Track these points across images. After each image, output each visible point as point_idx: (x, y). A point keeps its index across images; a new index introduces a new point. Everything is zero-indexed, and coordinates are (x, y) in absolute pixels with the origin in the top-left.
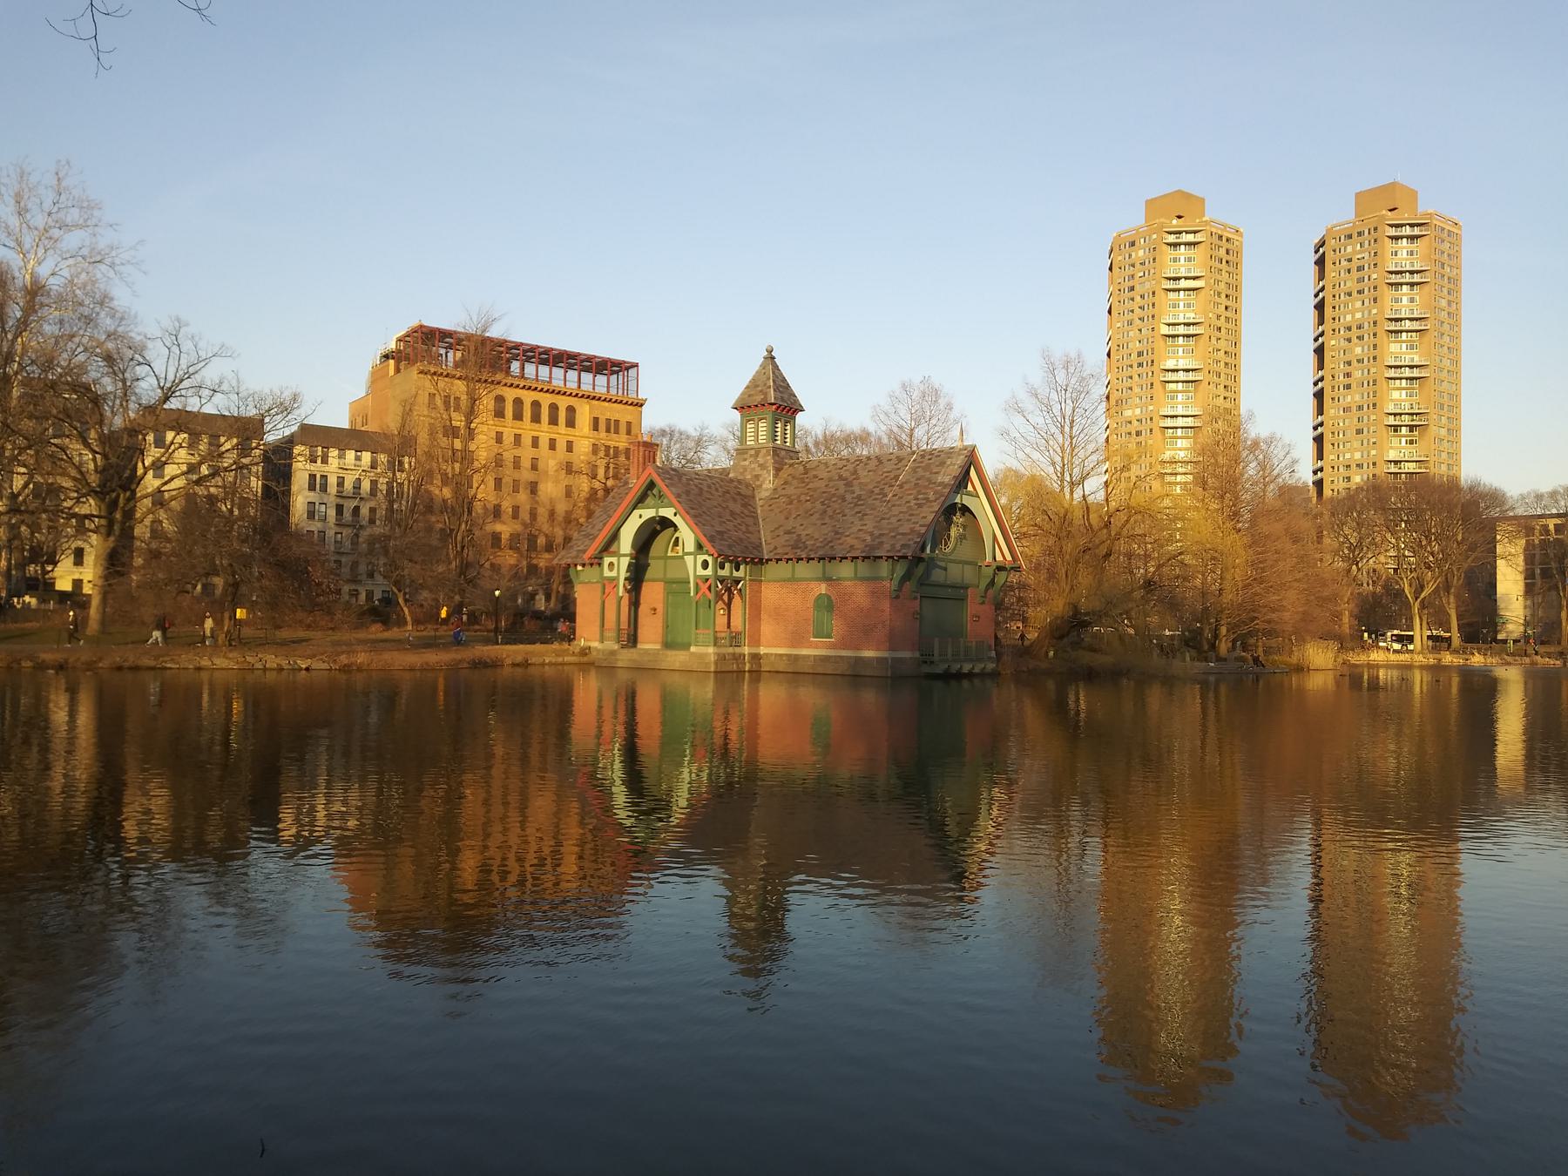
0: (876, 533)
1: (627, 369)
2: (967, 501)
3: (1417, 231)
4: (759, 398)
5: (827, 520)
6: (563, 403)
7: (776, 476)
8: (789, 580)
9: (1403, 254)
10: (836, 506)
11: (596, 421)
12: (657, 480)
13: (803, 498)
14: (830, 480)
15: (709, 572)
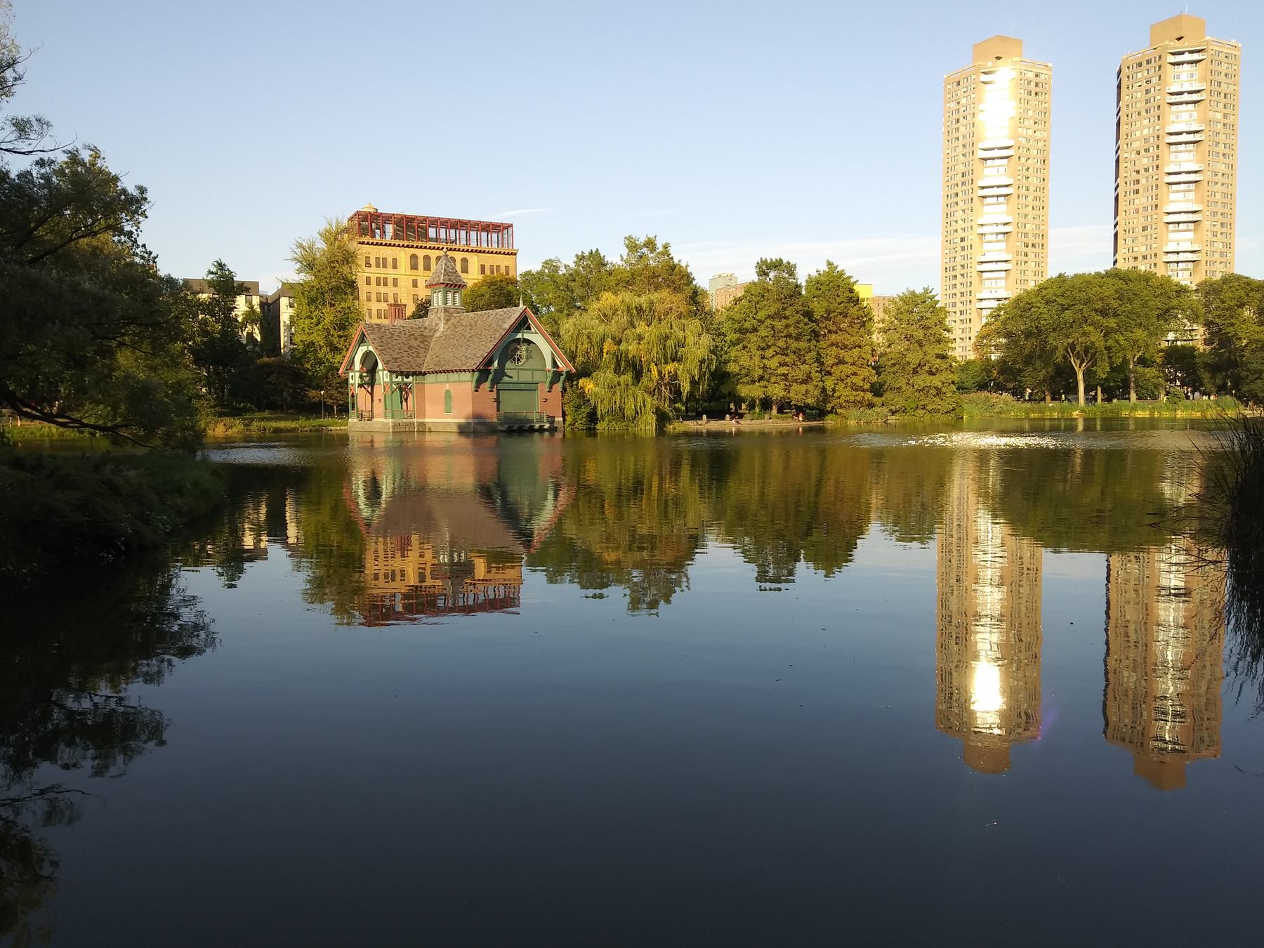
2: (527, 336)
3: (1196, 57)
9: (1184, 77)
11: (483, 267)
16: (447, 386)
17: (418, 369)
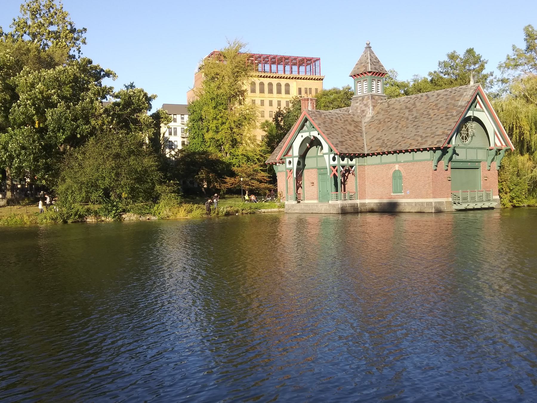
0: (424, 135)
1: (315, 61)
2: (477, 114)
4: (362, 70)
5: (398, 131)
6: (283, 82)
7: (373, 110)
8: (379, 164)
10: (403, 123)
11: (300, 90)
12: (309, 118)
13: (387, 120)
14: (401, 109)
15: (336, 162)
16: (397, 167)
17: (361, 152)
